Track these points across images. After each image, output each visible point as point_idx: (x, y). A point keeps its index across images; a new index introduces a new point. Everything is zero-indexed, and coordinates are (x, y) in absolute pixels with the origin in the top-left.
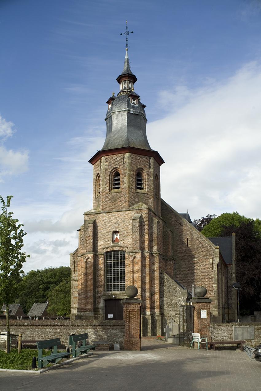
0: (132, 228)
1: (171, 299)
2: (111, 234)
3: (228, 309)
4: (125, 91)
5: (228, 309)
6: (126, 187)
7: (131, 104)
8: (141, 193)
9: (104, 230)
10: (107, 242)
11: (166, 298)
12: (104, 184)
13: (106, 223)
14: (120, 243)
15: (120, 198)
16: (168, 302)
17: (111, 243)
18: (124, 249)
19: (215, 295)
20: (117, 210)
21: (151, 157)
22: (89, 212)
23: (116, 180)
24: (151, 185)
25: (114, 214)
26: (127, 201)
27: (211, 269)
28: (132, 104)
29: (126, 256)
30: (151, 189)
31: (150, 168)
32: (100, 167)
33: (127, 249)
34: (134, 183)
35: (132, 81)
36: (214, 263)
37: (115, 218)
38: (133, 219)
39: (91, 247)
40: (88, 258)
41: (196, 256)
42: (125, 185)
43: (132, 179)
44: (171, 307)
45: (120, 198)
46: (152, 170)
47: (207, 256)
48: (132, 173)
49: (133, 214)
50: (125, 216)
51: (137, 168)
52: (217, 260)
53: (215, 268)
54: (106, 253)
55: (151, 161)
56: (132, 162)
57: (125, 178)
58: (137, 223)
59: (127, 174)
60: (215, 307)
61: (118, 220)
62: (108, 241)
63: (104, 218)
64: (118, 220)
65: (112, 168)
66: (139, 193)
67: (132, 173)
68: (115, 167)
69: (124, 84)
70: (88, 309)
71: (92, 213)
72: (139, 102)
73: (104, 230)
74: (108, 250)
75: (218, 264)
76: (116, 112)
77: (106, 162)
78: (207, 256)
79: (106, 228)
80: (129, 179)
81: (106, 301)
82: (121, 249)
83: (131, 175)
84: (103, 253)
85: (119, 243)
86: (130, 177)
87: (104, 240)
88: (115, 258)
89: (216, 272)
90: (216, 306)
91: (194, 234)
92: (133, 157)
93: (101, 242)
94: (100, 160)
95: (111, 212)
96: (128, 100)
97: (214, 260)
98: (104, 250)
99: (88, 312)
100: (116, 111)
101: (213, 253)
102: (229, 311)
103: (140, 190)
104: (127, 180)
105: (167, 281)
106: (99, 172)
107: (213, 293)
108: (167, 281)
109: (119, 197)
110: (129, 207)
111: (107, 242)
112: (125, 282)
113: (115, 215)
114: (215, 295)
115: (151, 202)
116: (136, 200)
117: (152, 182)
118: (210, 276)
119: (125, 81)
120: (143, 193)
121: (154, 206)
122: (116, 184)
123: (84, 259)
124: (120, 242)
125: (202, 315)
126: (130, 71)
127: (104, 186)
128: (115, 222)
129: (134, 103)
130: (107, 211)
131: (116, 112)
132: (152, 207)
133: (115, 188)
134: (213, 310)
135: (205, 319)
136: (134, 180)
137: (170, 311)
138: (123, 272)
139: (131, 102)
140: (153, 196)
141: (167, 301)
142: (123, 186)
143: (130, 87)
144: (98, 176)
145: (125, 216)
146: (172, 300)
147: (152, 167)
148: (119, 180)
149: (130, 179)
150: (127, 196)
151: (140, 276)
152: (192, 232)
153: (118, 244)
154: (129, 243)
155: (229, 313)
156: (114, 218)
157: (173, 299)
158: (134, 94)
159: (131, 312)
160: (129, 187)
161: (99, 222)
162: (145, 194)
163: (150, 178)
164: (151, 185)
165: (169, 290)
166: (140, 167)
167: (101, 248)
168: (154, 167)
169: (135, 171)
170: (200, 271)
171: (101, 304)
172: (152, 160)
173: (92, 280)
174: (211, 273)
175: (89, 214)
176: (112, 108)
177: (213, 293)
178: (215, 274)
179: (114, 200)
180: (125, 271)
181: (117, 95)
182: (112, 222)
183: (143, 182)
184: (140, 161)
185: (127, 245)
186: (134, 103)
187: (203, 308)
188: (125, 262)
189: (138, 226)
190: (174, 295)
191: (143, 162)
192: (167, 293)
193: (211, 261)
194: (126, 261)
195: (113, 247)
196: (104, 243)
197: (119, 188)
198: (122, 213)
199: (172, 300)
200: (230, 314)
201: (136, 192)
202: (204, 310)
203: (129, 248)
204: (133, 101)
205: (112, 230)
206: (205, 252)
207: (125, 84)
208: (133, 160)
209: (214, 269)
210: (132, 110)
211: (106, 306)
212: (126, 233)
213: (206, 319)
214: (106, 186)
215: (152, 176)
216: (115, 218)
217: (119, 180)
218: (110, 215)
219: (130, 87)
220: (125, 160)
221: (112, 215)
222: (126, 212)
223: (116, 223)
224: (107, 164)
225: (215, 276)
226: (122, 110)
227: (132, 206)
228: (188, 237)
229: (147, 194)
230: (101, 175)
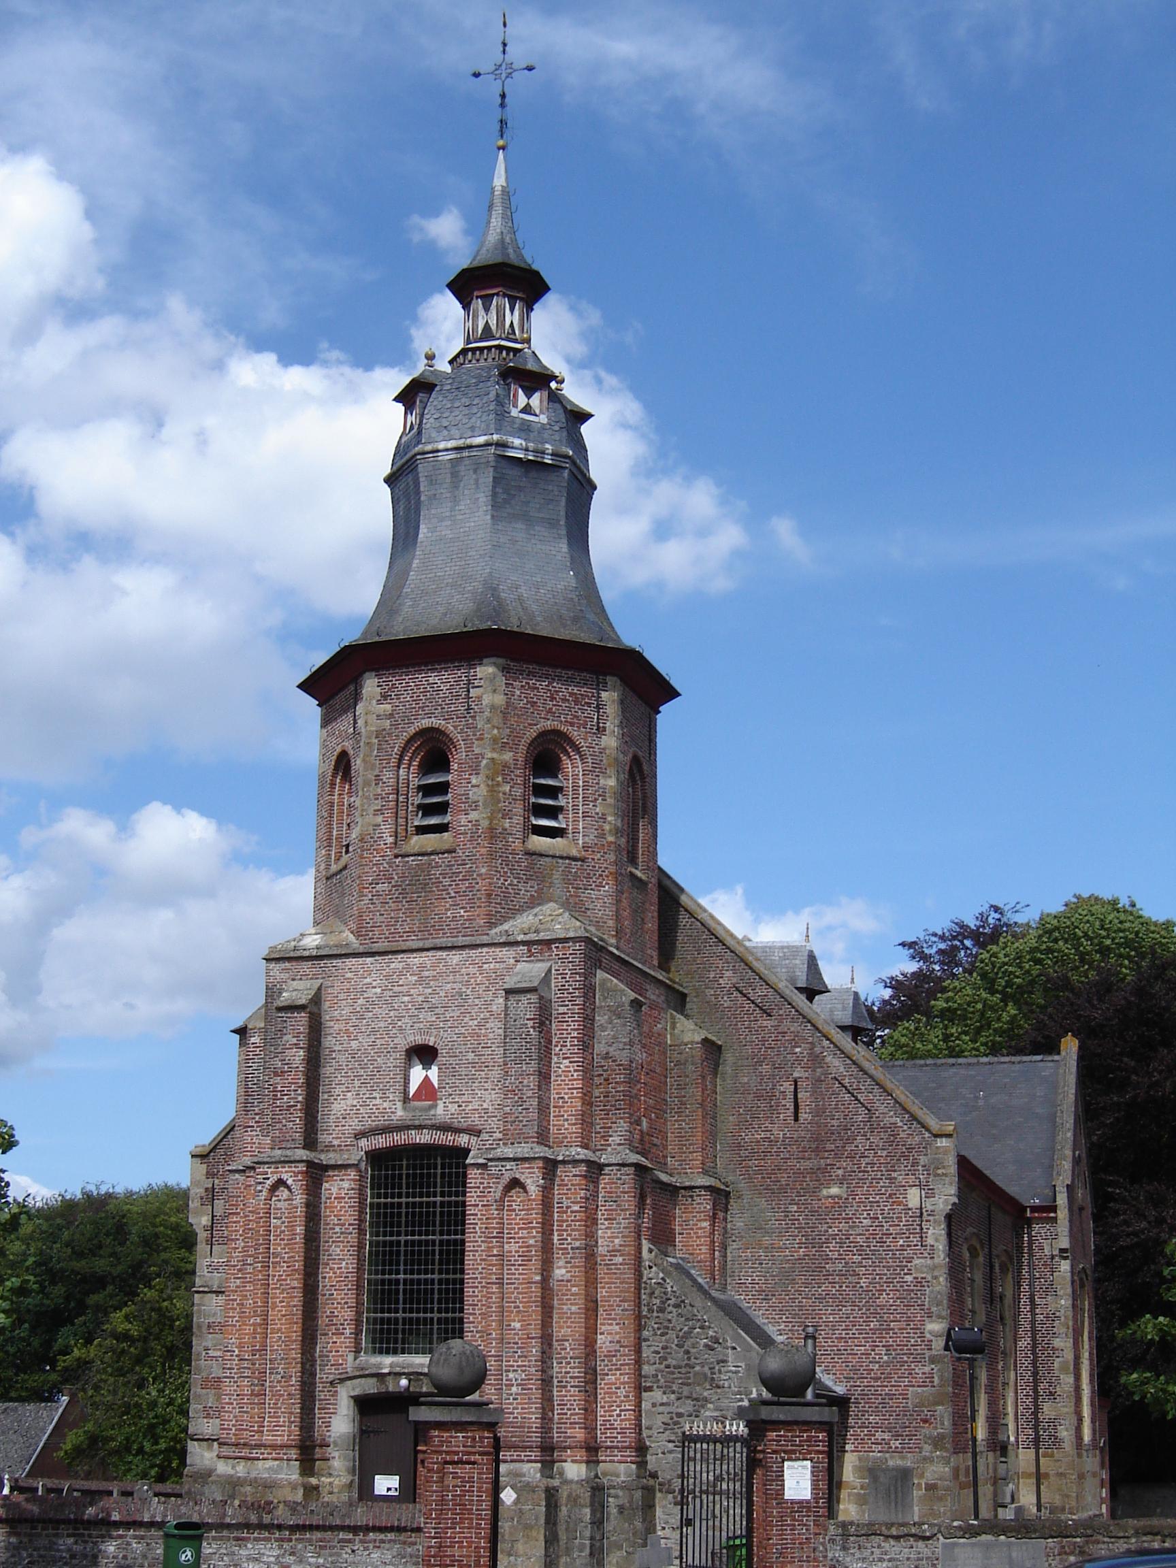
0: (501, 1032)
1: (697, 1399)
2: (398, 1058)
3: (1037, 1449)
4: (489, 348)
5: (1037, 1449)
6: (477, 824)
7: (514, 412)
8: (553, 857)
9: (365, 1041)
10: (378, 1101)
11: (673, 1392)
12: (371, 811)
13: (375, 1005)
14: (440, 1109)
16: (680, 1415)
17: (399, 1105)
18: (463, 1140)
19: (936, 1380)
20: (428, 944)
21: (611, 680)
22: (293, 944)
23: (427, 790)
25: (416, 960)
26: (482, 895)
27: (915, 1240)
28: (521, 412)
29: (473, 1174)
30: (602, 836)
31: (601, 730)
32: (355, 722)
33: (474, 1140)
34: (518, 809)
35: (521, 299)
36: (930, 1208)
37: (421, 980)
38: (509, 992)
39: (295, 1124)
40: (281, 1183)
41: (840, 1172)
42: (474, 815)
43: (507, 788)
45: (447, 882)
46: (610, 741)
47: (894, 1175)
48: (508, 756)
49: (512, 961)
50: (472, 970)
51: (532, 733)
52: (946, 1196)
53: (936, 1235)
54: (376, 1158)
56: (508, 704)
57: (474, 781)
58: (525, 1007)
59: (484, 762)
60: (937, 1442)
61: (434, 993)
62: (384, 1098)
63: (366, 981)
64: (434, 993)
65: (412, 731)
66: (541, 855)
67: (508, 756)
68: (426, 723)
69: (482, 312)
70: (274, 1447)
71: (306, 953)
72: (555, 398)
73: (365, 1041)
74: (381, 1142)
75: (949, 1217)
76: (438, 451)
77: (385, 697)
78: (894, 1175)
79: (374, 1031)
80: (492, 790)
81: (365, 1405)
82: (448, 1139)
83: (505, 765)
84: (356, 1155)
85: (435, 1106)
86: (500, 779)
87: (363, 1090)
88: (418, 1189)
89: (941, 1257)
90: (941, 1437)
91: (828, 1059)
93: (349, 1102)
94: (352, 688)
95: (403, 951)
96: (498, 395)
97: (930, 1194)
98: (363, 1142)
99: (269, 1464)
100: (442, 446)
101: (923, 1160)
102: (1042, 1460)
103: (548, 839)
104: (483, 790)
105: (677, 1306)
106: (348, 745)
107: (927, 1369)
108: (677, 1306)
109: (444, 875)
110: (492, 925)
111: (378, 1101)
112: (462, 1310)
113: (422, 967)
114: (936, 1380)
115: (602, 898)
116: (527, 890)
117: (610, 801)
118: (909, 1278)
119: (487, 300)
120: (562, 858)
121: (618, 918)
122: (428, 810)
123: (259, 1188)
124: (440, 1104)
125: (789, 1482)
126: (517, 249)
127: (372, 818)
128: (421, 998)
129: (527, 410)
130: (381, 946)
131: (438, 451)
132: (611, 923)
133: (422, 830)
134: (925, 1459)
135: (800, 1502)
136: (518, 792)
138: (455, 1255)
139: (515, 406)
140: (612, 869)
141: (673, 1409)
142: (463, 819)
143: (512, 324)
144: (343, 765)
145: (472, 970)
146: (703, 1406)
147: (612, 724)
148: (443, 788)
149: (498, 785)
150: (483, 871)
151: (538, 1278)
152: (818, 1050)
153: (432, 1112)
154: (486, 1111)
155: (1042, 1470)
156: (415, 978)
157: (706, 1400)
158: (531, 366)
159: (450, 1468)
160: (491, 829)
161: (342, 996)
162: (575, 859)
163: (602, 782)
165: (687, 1352)
166: (549, 724)
167: (349, 1130)
168: (621, 726)
169: (523, 748)
170: (861, 1250)
171: (340, 1422)
172: (610, 697)
173: (298, 1294)
174: (916, 1261)
175: (292, 954)
176: (419, 433)
177: (927, 1369)
178: (934, 1268)
179: (416, 886)
180: (463, 1251)
181: (451, 362)
182: (406, 999)
183: (562, 801)
184: (552, 699)
185: (475, 1120)
186: (527, 410)
187: (794, 1452)
188: (464, 1204)
189: (530, 1023)
190: (713, 1379)
192: (675, 1367)
193: (914, 1198)
194: (472, 1198)
195: (408, 1128)
196: (359, 1108)
197: (442, 828)
198: (455, 958)
199: (701, 1402)
200: (1047, 1475)
201: (526, 854)
202: (798, 1459)
203: (484, 1136)
204: (522, 400)
205: (403, 1042)
206: (885, 1153)
207: (487, 309)
208: (518, 693)
209: (930, 1241)
210: (517, 442)
211: (364, 1436)
212: (471, 1056)
213: (808, 1502)
214: (379, 819)
215: (611, 771)
216: (421, 980)
217: (443, 788)
218: (397, 963)
219: (512, 324)
220: (473, 692)
221: (408, 967)
222: (473, 953)
223: (425, 1005)
224: (388, 707)
225: (936, 1278)
226: (469, 441)
227: (505, 919)
228: (796, 1075)
229: (583, 860)
230: (357, 764)
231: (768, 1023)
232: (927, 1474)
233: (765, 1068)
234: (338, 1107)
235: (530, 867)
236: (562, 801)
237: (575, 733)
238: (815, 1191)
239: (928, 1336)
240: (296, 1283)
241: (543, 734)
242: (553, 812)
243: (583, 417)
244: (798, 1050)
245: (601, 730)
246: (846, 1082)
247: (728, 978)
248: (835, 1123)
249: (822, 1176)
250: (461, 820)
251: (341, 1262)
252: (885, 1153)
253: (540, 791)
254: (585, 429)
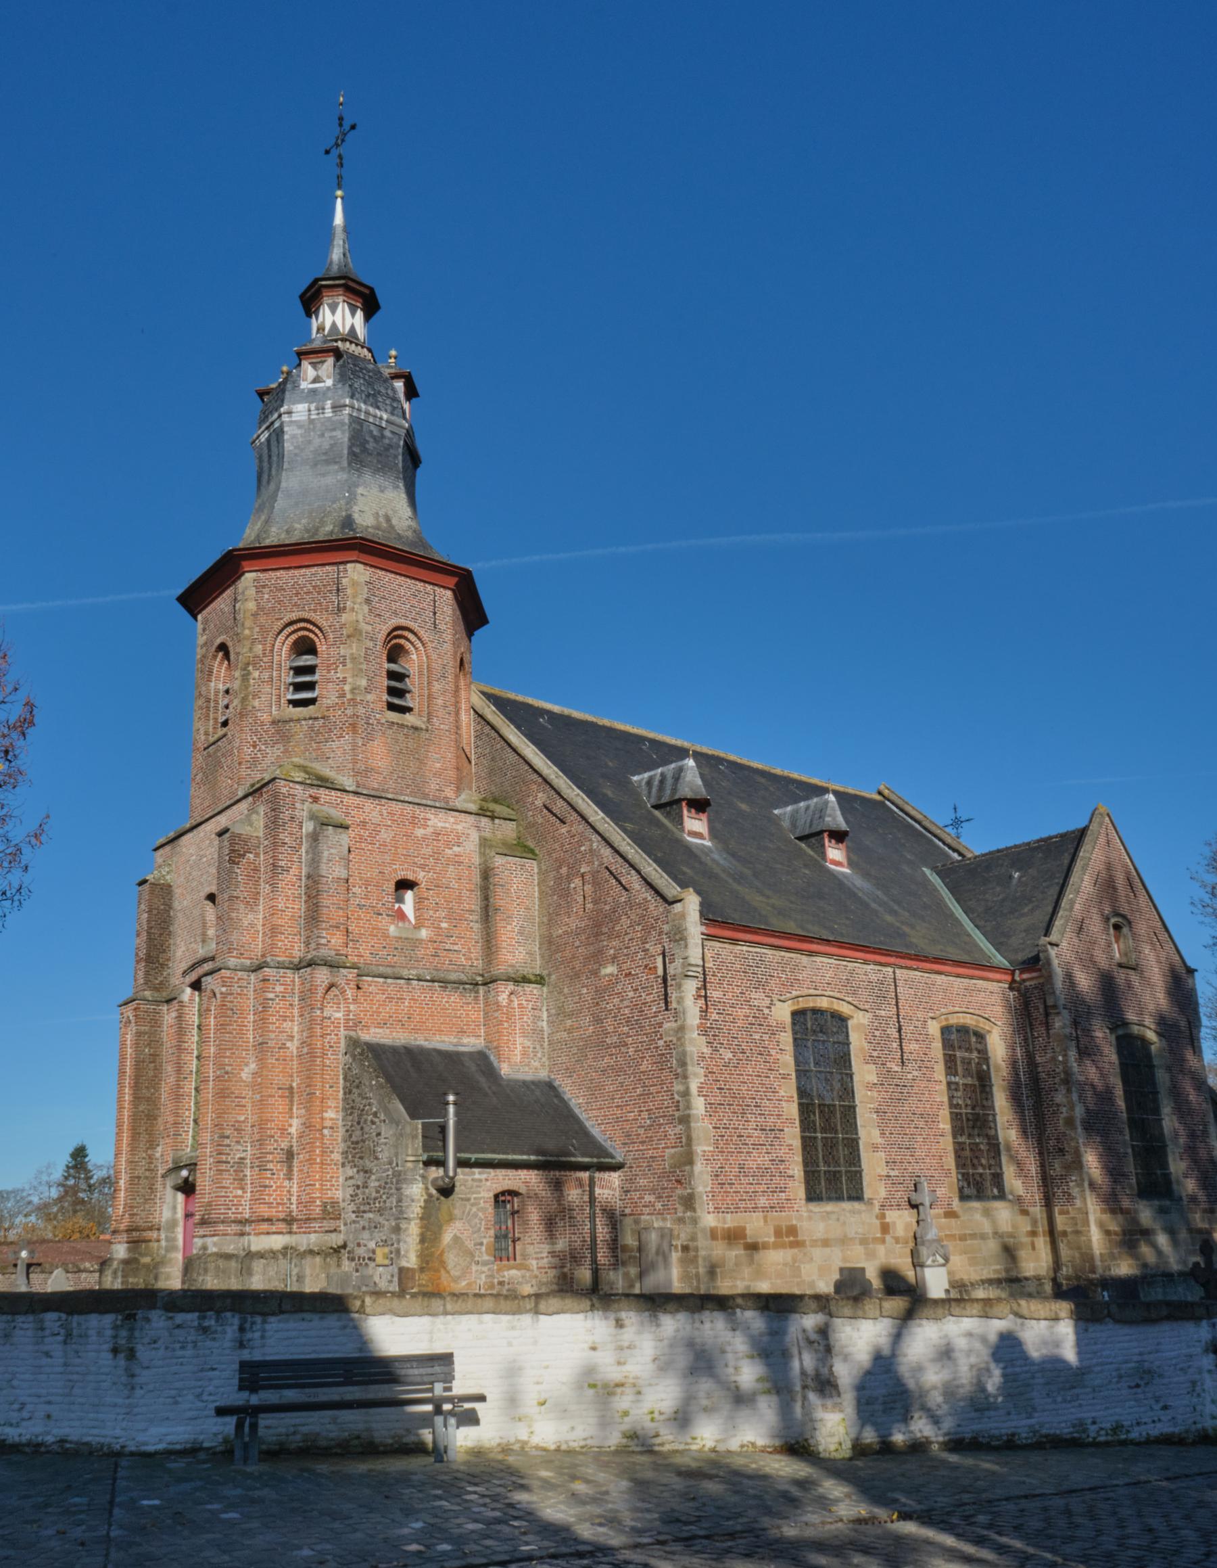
15: (223, 760)
24: (344, 680)
44: (364, 1212)
47: (647, 946)
55: (344, 581)
78: (647, 946)
92: (263, 587)
118: (661, 1043)
137: (364, 1228)
164: (344, 680)
165: (362, 1128)
174: (666, 1026)
177: (677, 1130)
183: (316, 677)
186: (317, 380)
191: (308, 593)
206: (640, 927)
220: (238, 605)
228: (582, 870)
231: (564, 830)
232: (683, 1235)
233: (564, 870)
234: (179, 953)
235: (278, 732)
236: (316, 677)
238: (595, 973)
239: (676, 1096)
242: (310, 686)
244: (583, 848)
245: (340, 610)
246: (613, 869)
247: (541, 798)
248: (607, 907)
249: (598, 957)
252: (640, 927)
253: (299, 671)
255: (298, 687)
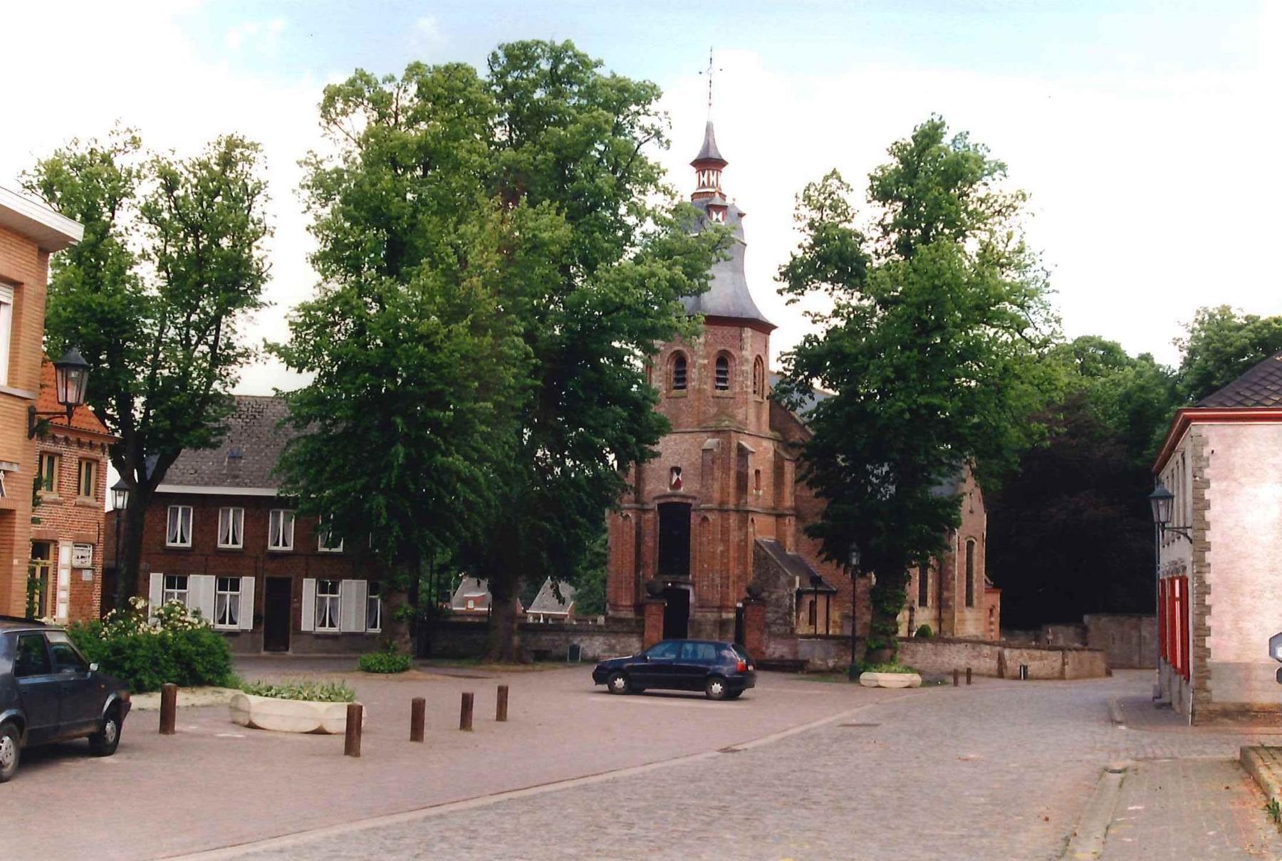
18: (690, 501)
34: (710, 381)
38: (704, 450)
51: (715, 352)
74: (662, 501)
82: (685, 501)
129: (717, 220)
133: (676, 388)
197: (684, 387)
198: (687, 436)
234: (648, 488)
237: (732, 351)
240: (633, 550)
241: (720, 351)
242: (725, 380)
243: (741, 215)
250: (692, 384)
251: (650, 542)
254: (744, 220)
255: (718, 380)
